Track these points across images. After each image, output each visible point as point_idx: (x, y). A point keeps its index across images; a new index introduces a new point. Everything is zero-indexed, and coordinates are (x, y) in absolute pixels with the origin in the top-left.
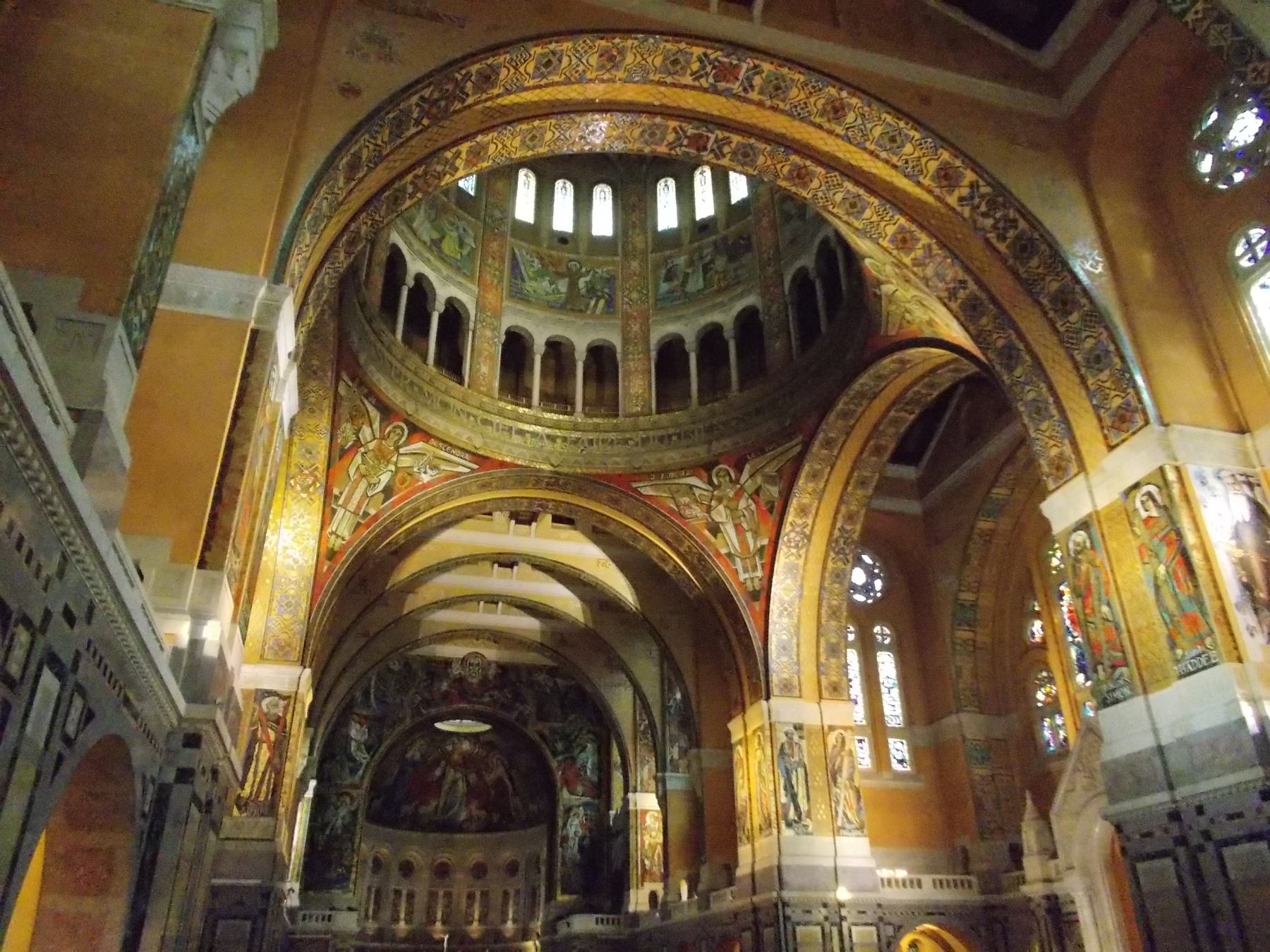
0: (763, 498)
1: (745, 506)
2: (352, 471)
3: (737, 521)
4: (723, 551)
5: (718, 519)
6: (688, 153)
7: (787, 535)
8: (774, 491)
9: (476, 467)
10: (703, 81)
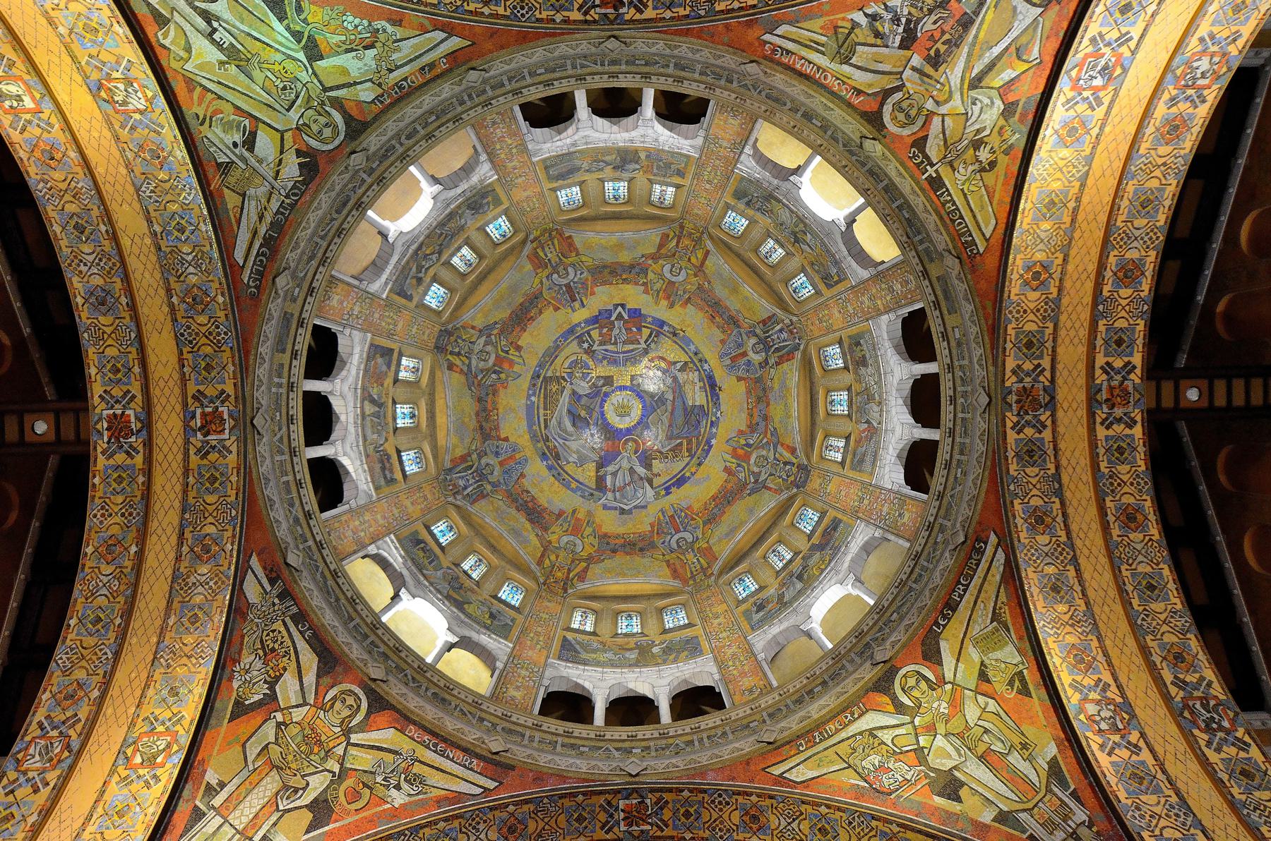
0: (999, 682)
1: (978, 712)
2: (252, 751)
3: (981, 748)
4: (987, 817)
5: (947, 764)
6: (605, 15)
7: (1081, 710)
8: (1009, 656)
9: (491, 785)
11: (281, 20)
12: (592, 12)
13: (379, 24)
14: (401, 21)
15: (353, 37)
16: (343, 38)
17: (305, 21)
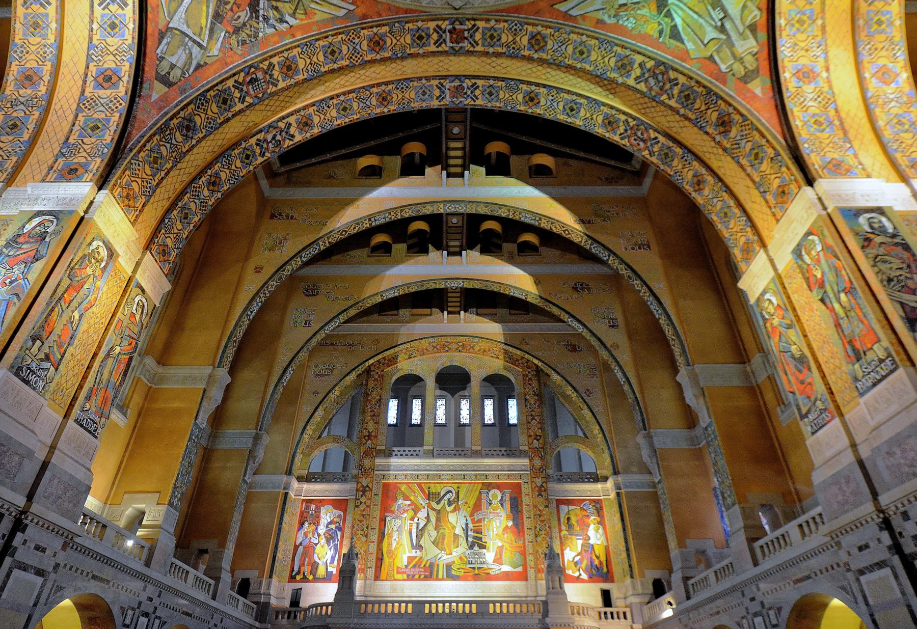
6: (461, 24)
10: (470, 84)
11: (676, 26)
12: (470, 26)
13: (613, 21)
14: (597, 22)
15: (632, 12)
16: (638, 12)
17: (660, 24)
